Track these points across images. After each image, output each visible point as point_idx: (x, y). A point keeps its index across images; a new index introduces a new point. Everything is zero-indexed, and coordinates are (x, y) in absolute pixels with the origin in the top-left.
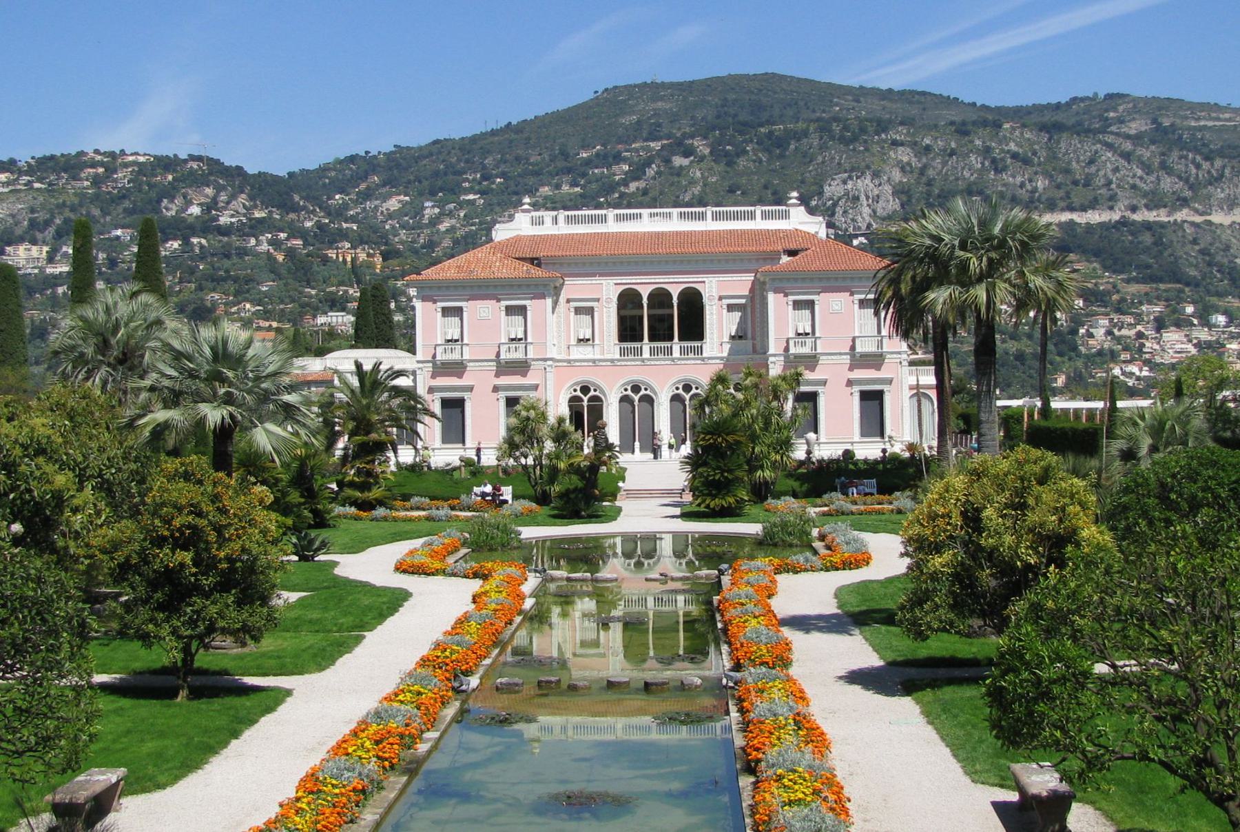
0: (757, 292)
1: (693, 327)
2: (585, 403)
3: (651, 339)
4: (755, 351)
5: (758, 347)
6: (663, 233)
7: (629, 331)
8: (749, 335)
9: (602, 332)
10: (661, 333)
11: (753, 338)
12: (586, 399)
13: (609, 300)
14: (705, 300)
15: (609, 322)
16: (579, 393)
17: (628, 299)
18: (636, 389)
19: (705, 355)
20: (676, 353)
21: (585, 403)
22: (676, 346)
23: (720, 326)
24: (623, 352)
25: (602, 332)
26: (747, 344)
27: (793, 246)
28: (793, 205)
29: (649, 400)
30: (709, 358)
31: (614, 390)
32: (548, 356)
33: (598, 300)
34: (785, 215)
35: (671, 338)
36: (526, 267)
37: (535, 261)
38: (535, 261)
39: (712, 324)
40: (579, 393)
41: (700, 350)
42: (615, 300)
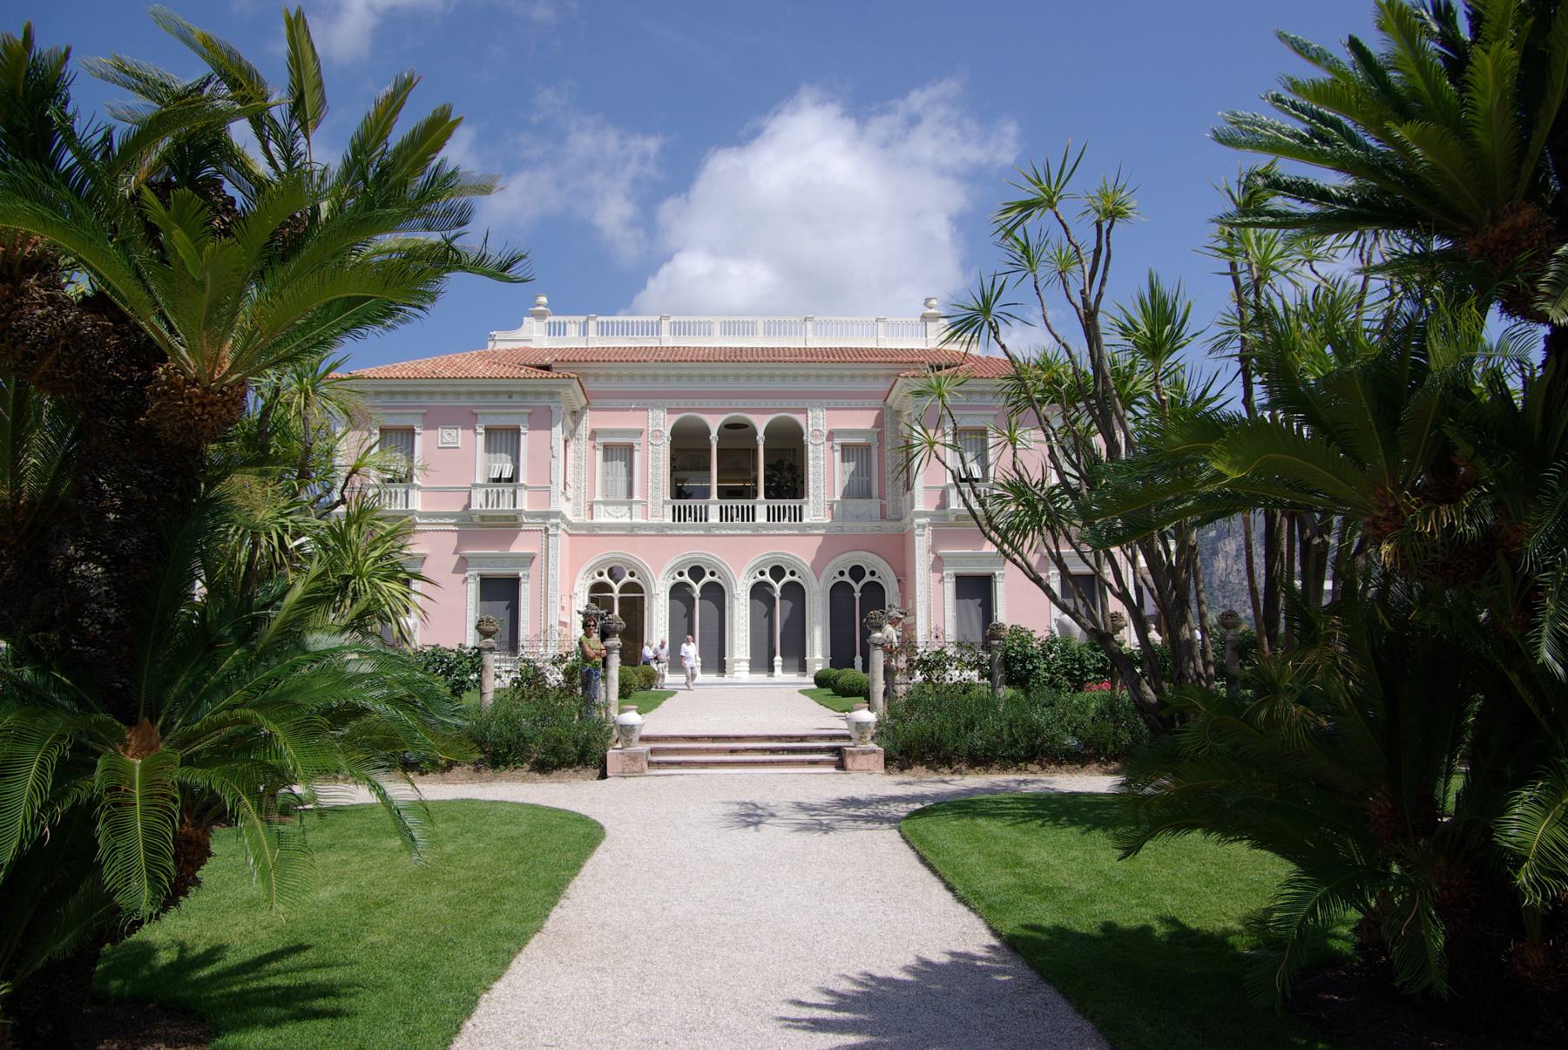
0: (888, 426)
1: (788, 479)
2: (616, 594)
3: (724, 493)
4: (883, 517)
5: (889, 512)
8: (875, 492)
9: (645, 481)
11: (882, 496)
12: (616, 588)
13: (657, 434)
14: (809, 438)
15: (656, 467)
16: (606, 578)
18: (696, 573)
19: (805, 520)
20: (761, 518)
21: (616, 594)
22: (761, 506)
23: (826, 474)
24: (678, 514)
25: (645, 481)
26: (873, 505)
29: (716, 594)
31: (663, 573)
32: (553, 508)
35: (755, 495)
37: (547, 368)
39: (816, 473)
40: (606, 578)
41: (798, 514)
42: (667, 433)
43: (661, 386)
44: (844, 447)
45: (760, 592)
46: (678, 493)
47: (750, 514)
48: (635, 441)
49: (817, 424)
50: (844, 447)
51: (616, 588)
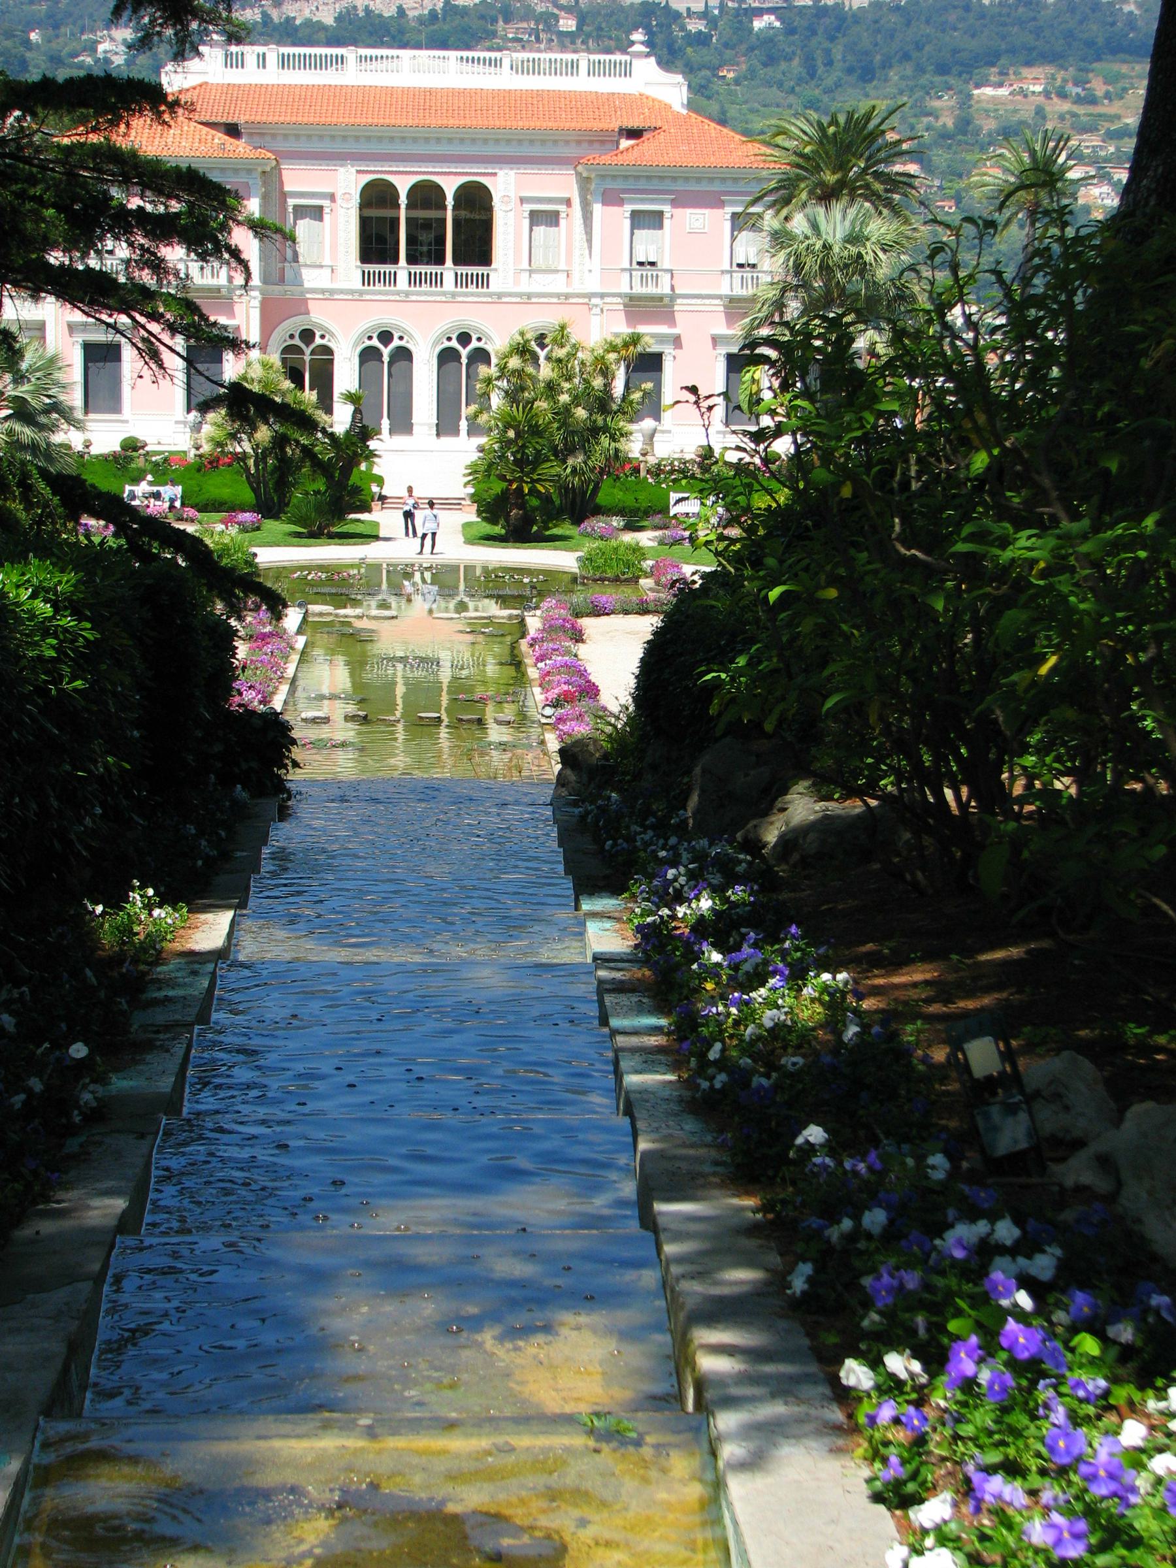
1: (476, 246)
2: (307, 358)
6: (430, 92)
7: (376, 245)
10: (426, 250)
12: (308, 351)
16: (297, 341)
17: (377, 196)
19: (494, 287)
21: (307, 358)
22: (449, 270)
24: (367, 279)
27: (634, 123)
28: (638, 55)
30: (500, 295)
33: (332, 197)
34: (627, 71)
35: (440, 261)
36: (220, 137)
37: (233, 130)
38: (233, 130)
40: (297, 341)
41: (483, 281)
43: (351, 147)
44: (533, 214)
45: (447, 357)
46: (367, 255)
47: (438, 280)
48: (325, 203)
49: (508, 189)
50: (533, 214)
51: (308, 351)
